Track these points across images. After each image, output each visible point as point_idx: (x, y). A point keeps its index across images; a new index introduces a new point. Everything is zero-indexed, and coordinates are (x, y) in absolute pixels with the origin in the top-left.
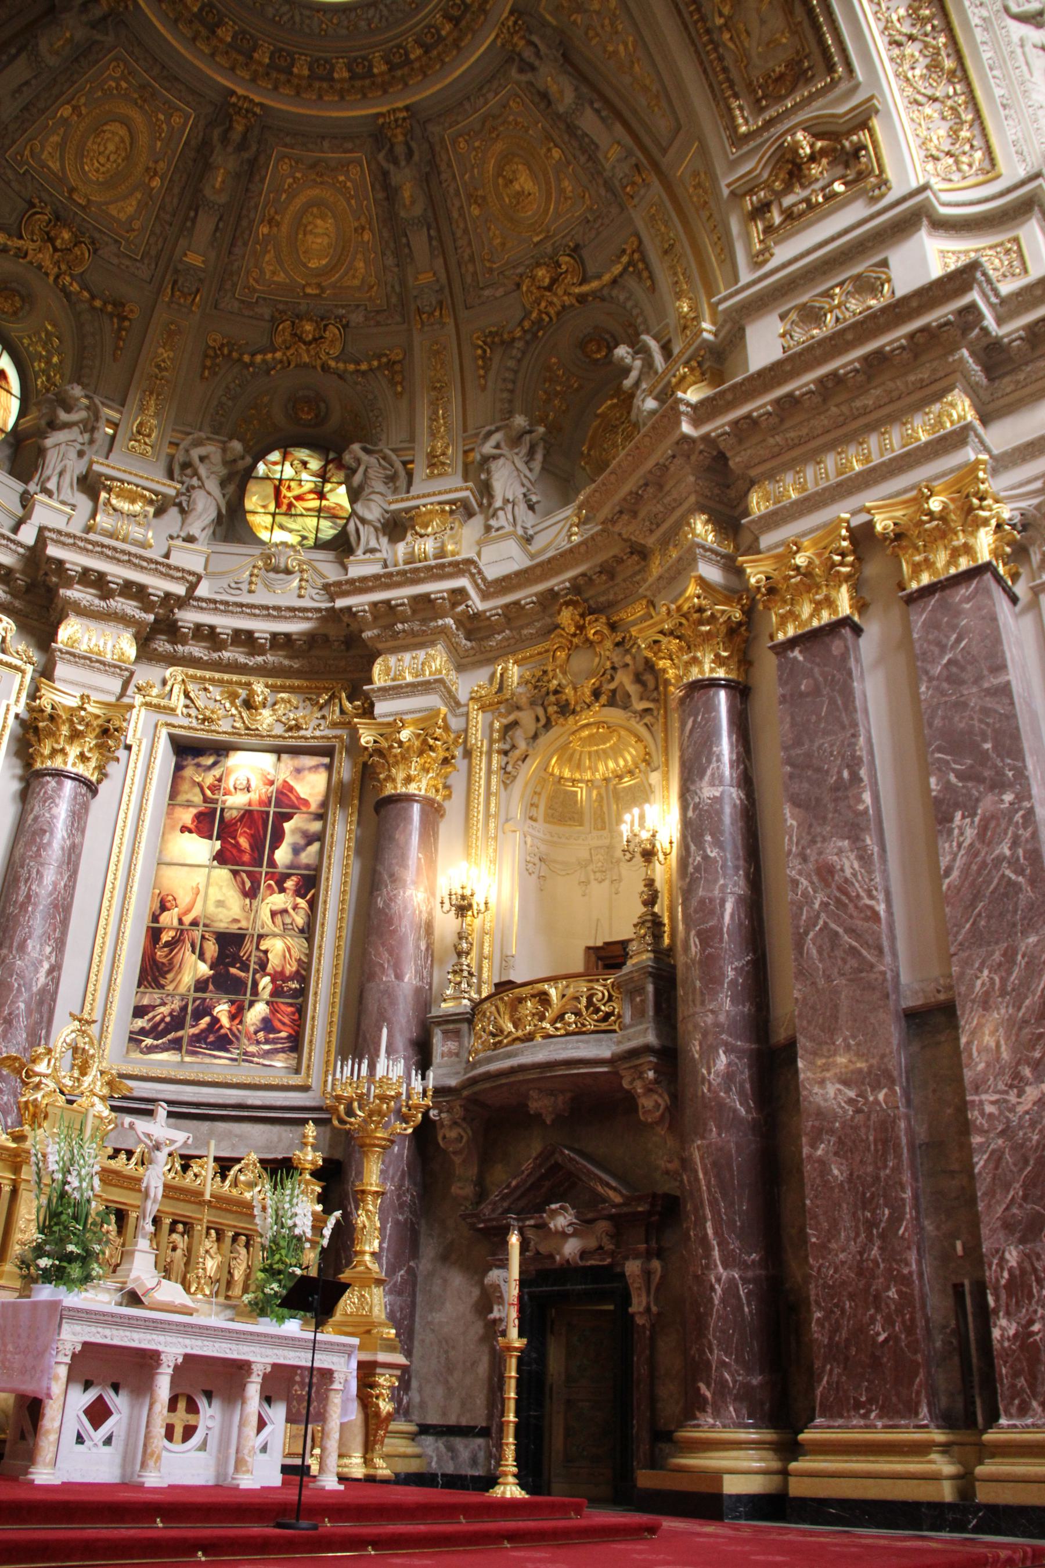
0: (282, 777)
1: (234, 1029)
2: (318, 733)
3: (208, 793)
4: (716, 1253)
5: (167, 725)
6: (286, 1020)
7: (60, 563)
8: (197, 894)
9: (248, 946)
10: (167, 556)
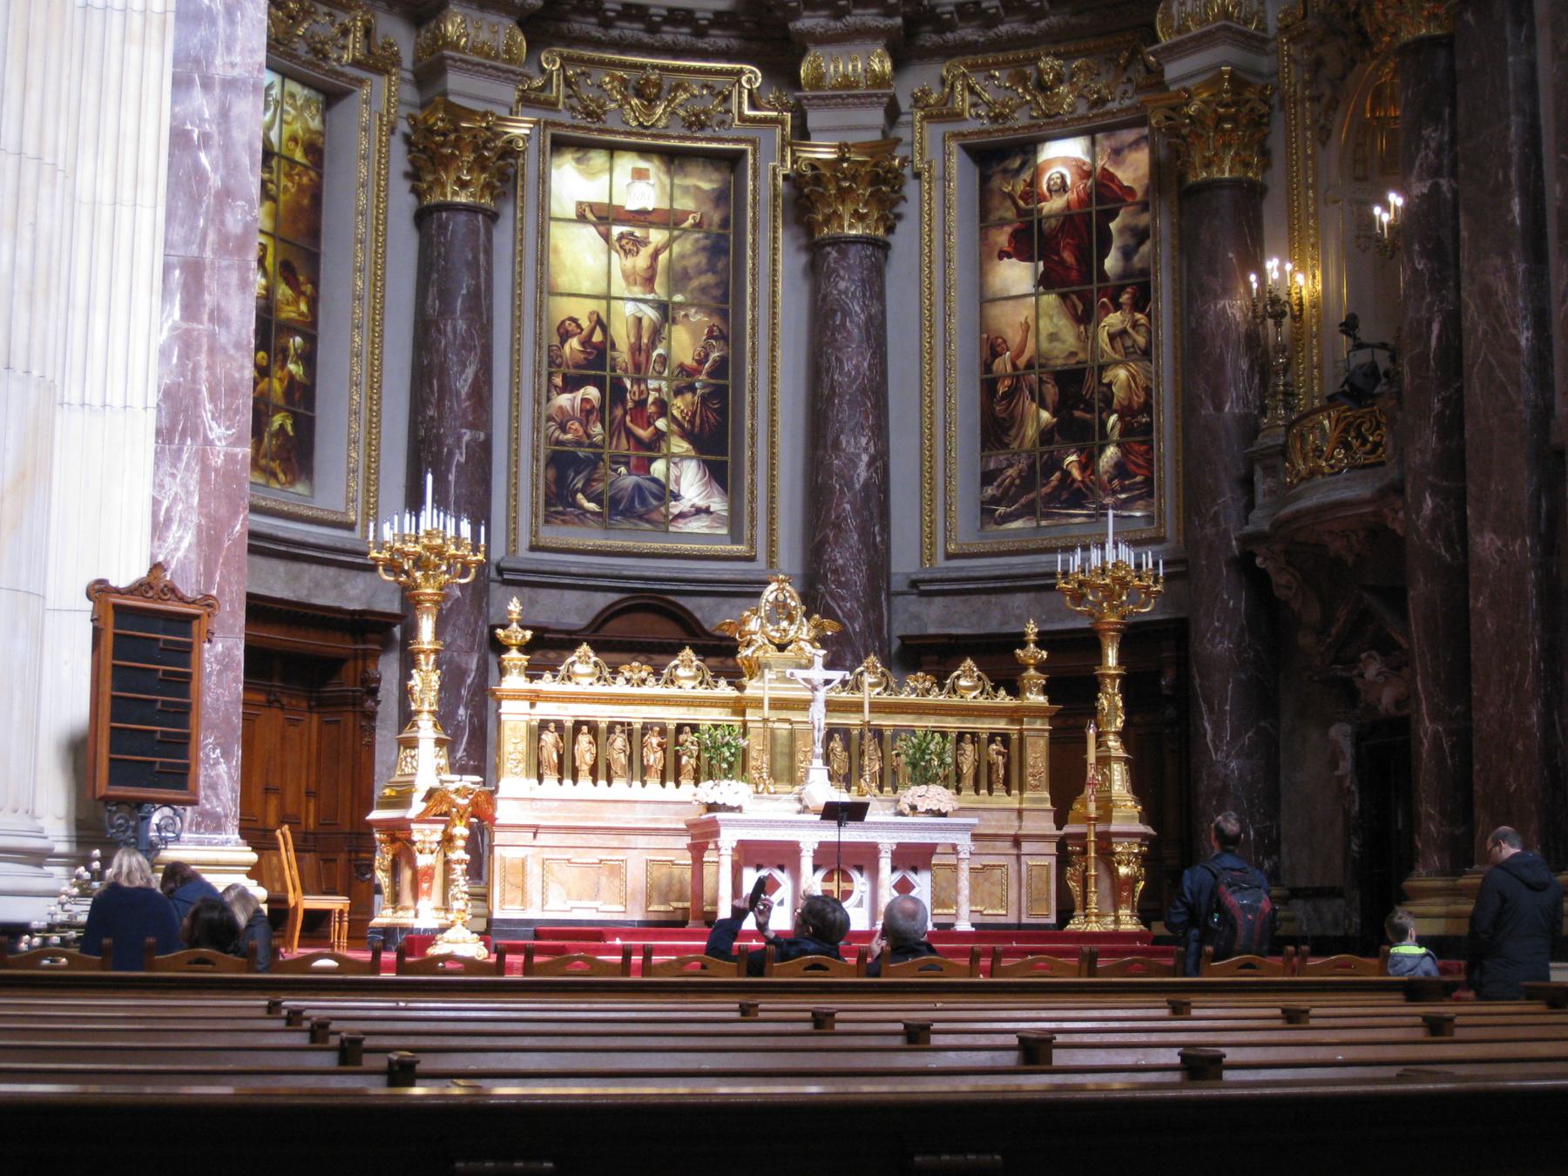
0: (1100, 163)
2: (1127, 103)
3: (1021, 203)
4: (1424, 707)
6: (1141, 462)
9: (1090, 382)
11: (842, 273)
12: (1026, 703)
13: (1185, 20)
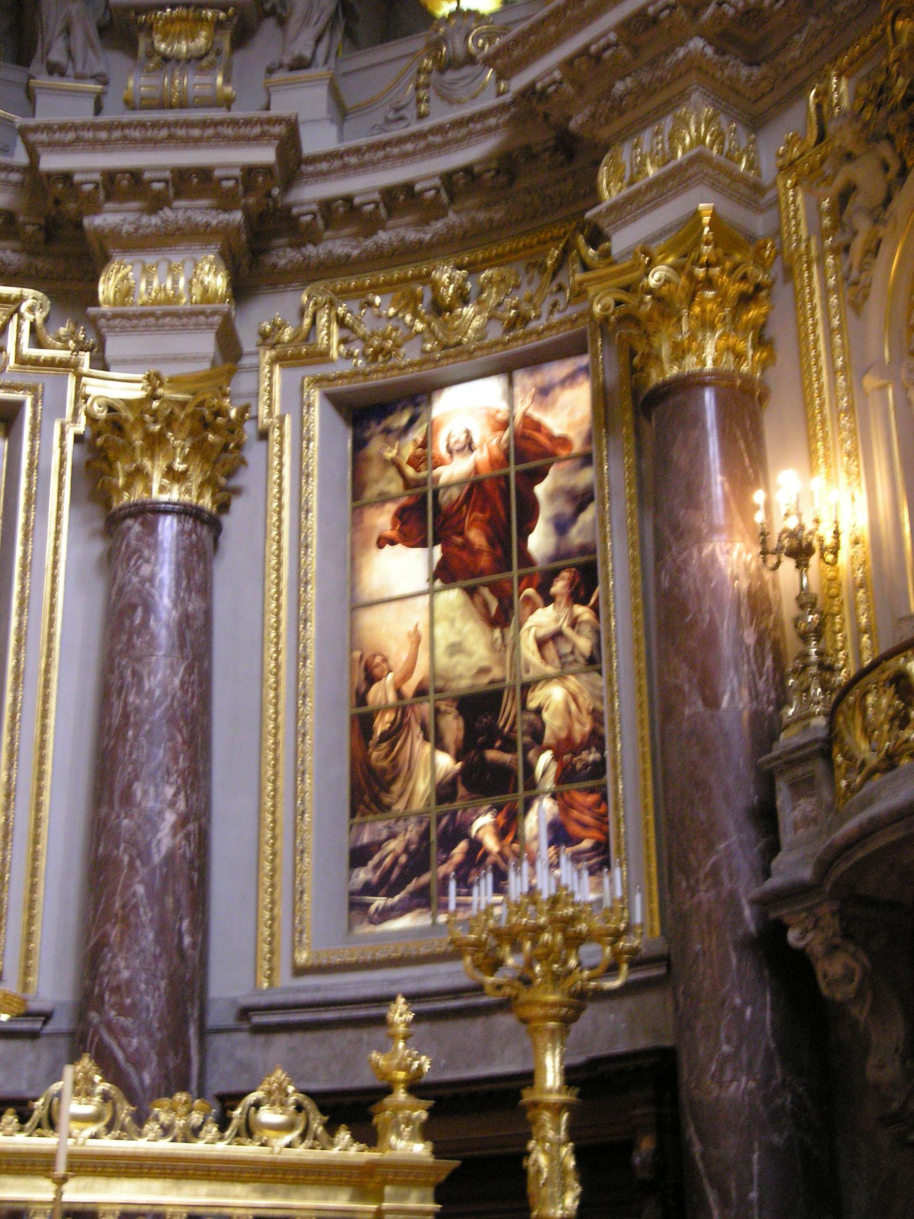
0: (519, 410)
1: (507, 851)
2: (556, 317)
3: (410, 471)
5: (318, 381)
6: (587, 818)
7: (66, 177)
8: (418, 642)
9: (509, 707)
10: (268, 108)
11: (146, 553)
12: (387, 1155)
13: (643, 164)
